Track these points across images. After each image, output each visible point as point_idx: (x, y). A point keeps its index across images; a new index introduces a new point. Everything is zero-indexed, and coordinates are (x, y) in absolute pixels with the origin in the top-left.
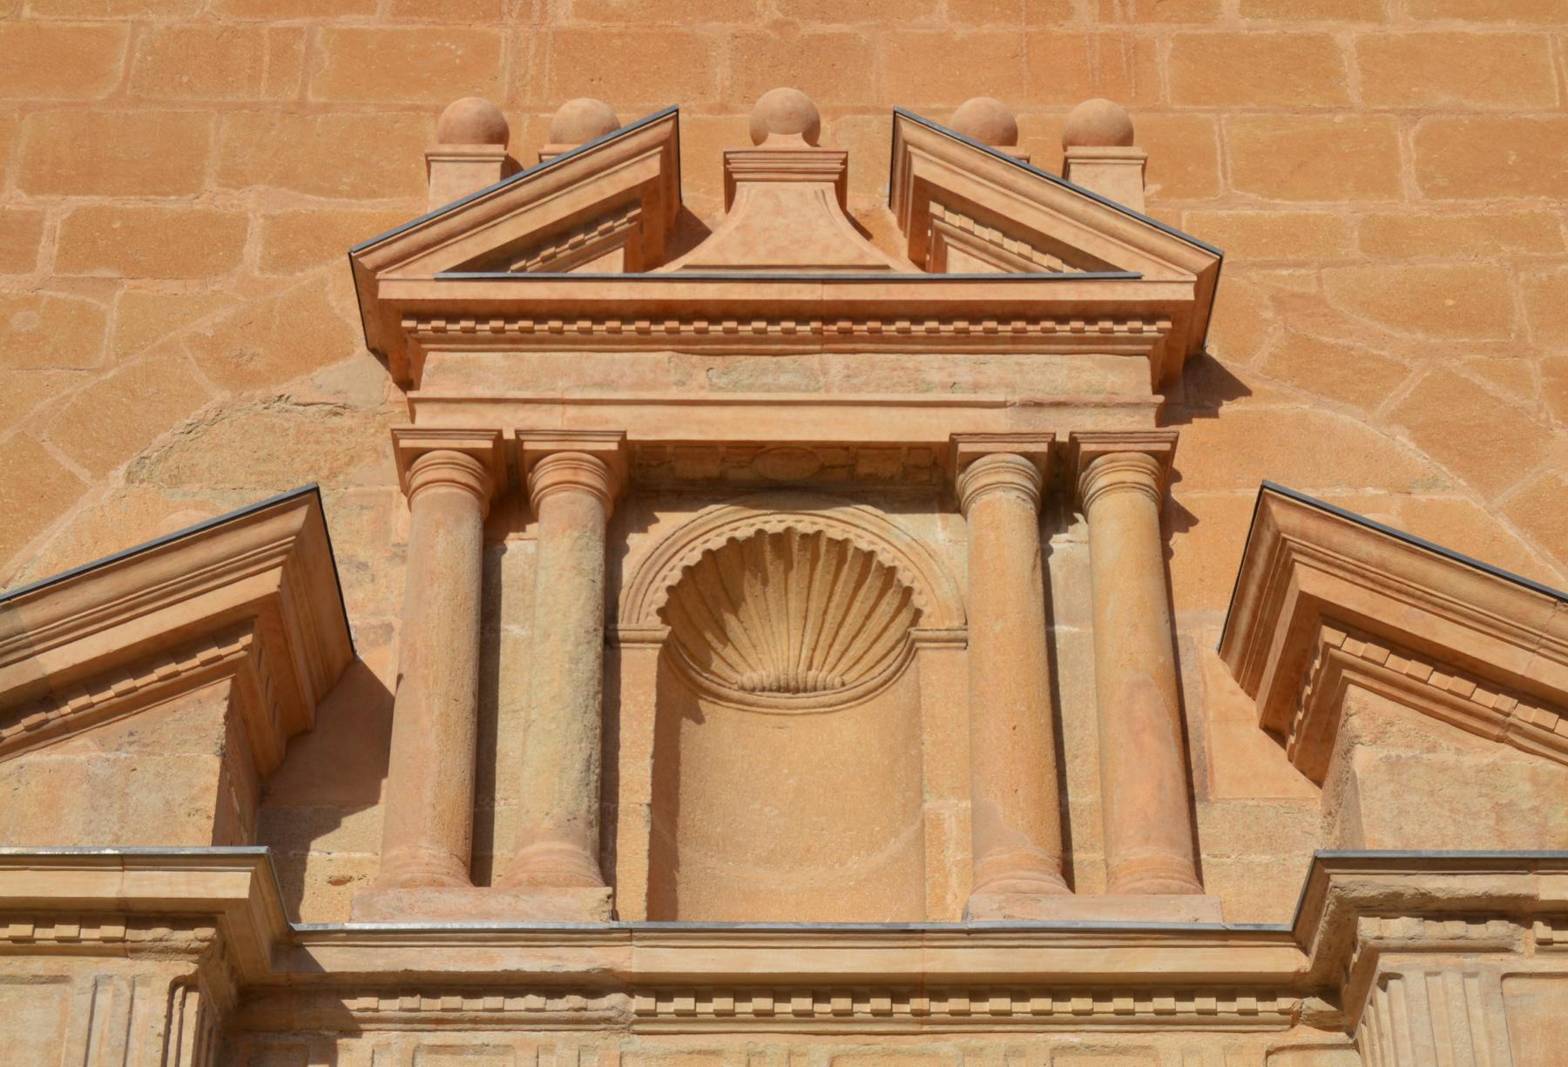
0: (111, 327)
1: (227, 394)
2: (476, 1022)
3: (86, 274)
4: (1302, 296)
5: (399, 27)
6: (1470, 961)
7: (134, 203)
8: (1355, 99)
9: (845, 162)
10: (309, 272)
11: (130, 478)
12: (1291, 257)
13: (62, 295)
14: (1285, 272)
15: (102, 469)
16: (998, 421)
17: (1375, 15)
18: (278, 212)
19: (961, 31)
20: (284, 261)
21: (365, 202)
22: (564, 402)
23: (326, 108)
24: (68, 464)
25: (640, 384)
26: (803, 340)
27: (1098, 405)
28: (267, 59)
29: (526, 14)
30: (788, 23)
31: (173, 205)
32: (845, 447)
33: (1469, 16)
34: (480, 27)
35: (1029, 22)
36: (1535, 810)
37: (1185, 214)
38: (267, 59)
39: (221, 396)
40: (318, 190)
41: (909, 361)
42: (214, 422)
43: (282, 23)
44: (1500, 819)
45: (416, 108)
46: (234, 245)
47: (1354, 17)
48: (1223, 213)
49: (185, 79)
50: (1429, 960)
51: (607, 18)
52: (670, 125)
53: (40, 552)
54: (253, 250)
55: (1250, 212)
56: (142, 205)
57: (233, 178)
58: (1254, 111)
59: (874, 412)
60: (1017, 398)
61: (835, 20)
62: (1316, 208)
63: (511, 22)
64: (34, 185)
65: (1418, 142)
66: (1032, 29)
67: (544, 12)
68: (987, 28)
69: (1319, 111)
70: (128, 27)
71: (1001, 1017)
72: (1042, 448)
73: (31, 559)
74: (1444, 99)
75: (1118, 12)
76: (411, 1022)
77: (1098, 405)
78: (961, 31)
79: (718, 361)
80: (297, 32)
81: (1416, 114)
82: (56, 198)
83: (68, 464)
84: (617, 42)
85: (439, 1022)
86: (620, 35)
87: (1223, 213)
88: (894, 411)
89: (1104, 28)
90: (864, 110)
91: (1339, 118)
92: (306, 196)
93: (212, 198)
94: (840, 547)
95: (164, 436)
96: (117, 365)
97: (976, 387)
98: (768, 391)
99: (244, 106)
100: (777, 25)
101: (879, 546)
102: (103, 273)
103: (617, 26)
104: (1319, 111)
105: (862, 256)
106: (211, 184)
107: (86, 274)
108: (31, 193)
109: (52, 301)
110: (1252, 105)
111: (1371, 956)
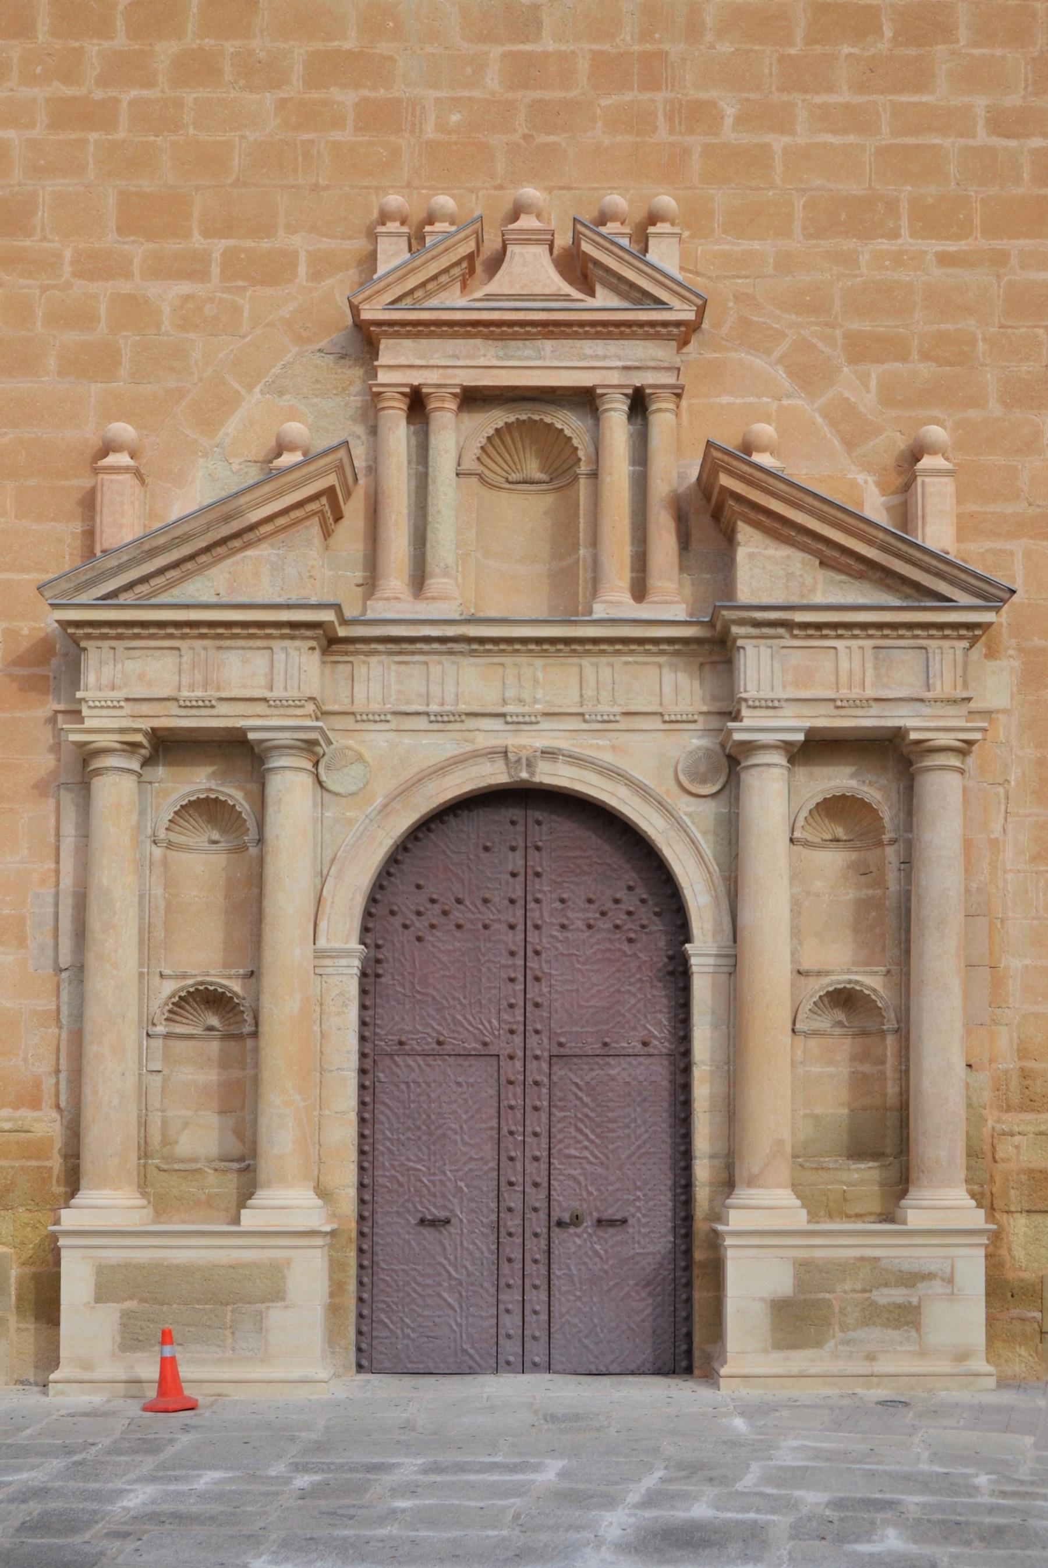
0: (246, 314)
1: (297, 349)
2: (413, 653)
3: (233, 284)
4: (746, 294)
5: (358, 139)
6: (769, 642)
7: (249, 244)
8: (778, 181)
9: (553, 235)
10: (327, 282)
11: (262, 392)
12: (744, 273)
13: (224, 296)
14: (740, 281)
15: (250, 388)
16: (615, 378)
17: (792, 132)
18: (310, 248)
19: (606, 141)
20: (316, 276)
21: (348, 242)
22: (438, 367)
23: (327, 188)
24: (236, 386)
25: (467, 357)
26: (534, 334)
27: (654, 368)
28: (300, 158)
29: (412, 131)
30: (531, 136)
31: (266, 245)
32: (552, 388)
33: (835, 132)
34: (393, 139)
35: (637, 135)
36: (801, 576)
37: (700, 249)
38: (300, 158)
39: (294, 350)
40: (327, 236)
41: (578, 343)
42: (292, 363)
43: (306, 137)
44: (788, 581)
45: (367, 187)
46: (294, 266)
47: (783, 132)
48: (716, 248)
49: (265, 171)
50: (754, 641)
51: (450, 133)
52: (479, 224)
53: (230, 431)
54: (302, 270)
55: (728, 247)
56: (253, 245)
57: (291, 229)
58: (732, 189)
59: (563, 371)
60: (620, 364)
61: (550, 134)
62: (756, 245)
63: (407, 135)
64: (207, 233)
65: (804, 207)
66: (639, 139)
67: (421, 129)
68: (619, 138)
69: (761, 189)
70: (237, 139)
71: (603, 652)
72: (630, 391)
73: (228, 434)
74: (818, 182)
75: (677, 130)
76: (391, 653)
77: (654, 368)
79: (500, 343)
80: (312, 141)
81: (804, 190)
82: (216, 241)
83: (236, 386)
84: (454, 147)
85: (400, 653)
86: (456, 143)
87: (716, 248)
88: (571, 372)
89: (671, 139)
90: (563, 188)
91: (770, 194)
92: (324, 239)
93: (282, 240)
94: (550, 426)
95: (273, 371)
96: (250, 333)
97: (605, 357)
98: (520, 359)
99: (292, 187)
100: (526, 137)
101: (565, 427)
102: (240, 283)
103: (454, 138)
104: (761, 189)
105: (560, 289)
106: (281, 232)
107: (233, 284)
108: (205, 238)
109: (221, 299)
110: (733, 185)
111: (735, 640)
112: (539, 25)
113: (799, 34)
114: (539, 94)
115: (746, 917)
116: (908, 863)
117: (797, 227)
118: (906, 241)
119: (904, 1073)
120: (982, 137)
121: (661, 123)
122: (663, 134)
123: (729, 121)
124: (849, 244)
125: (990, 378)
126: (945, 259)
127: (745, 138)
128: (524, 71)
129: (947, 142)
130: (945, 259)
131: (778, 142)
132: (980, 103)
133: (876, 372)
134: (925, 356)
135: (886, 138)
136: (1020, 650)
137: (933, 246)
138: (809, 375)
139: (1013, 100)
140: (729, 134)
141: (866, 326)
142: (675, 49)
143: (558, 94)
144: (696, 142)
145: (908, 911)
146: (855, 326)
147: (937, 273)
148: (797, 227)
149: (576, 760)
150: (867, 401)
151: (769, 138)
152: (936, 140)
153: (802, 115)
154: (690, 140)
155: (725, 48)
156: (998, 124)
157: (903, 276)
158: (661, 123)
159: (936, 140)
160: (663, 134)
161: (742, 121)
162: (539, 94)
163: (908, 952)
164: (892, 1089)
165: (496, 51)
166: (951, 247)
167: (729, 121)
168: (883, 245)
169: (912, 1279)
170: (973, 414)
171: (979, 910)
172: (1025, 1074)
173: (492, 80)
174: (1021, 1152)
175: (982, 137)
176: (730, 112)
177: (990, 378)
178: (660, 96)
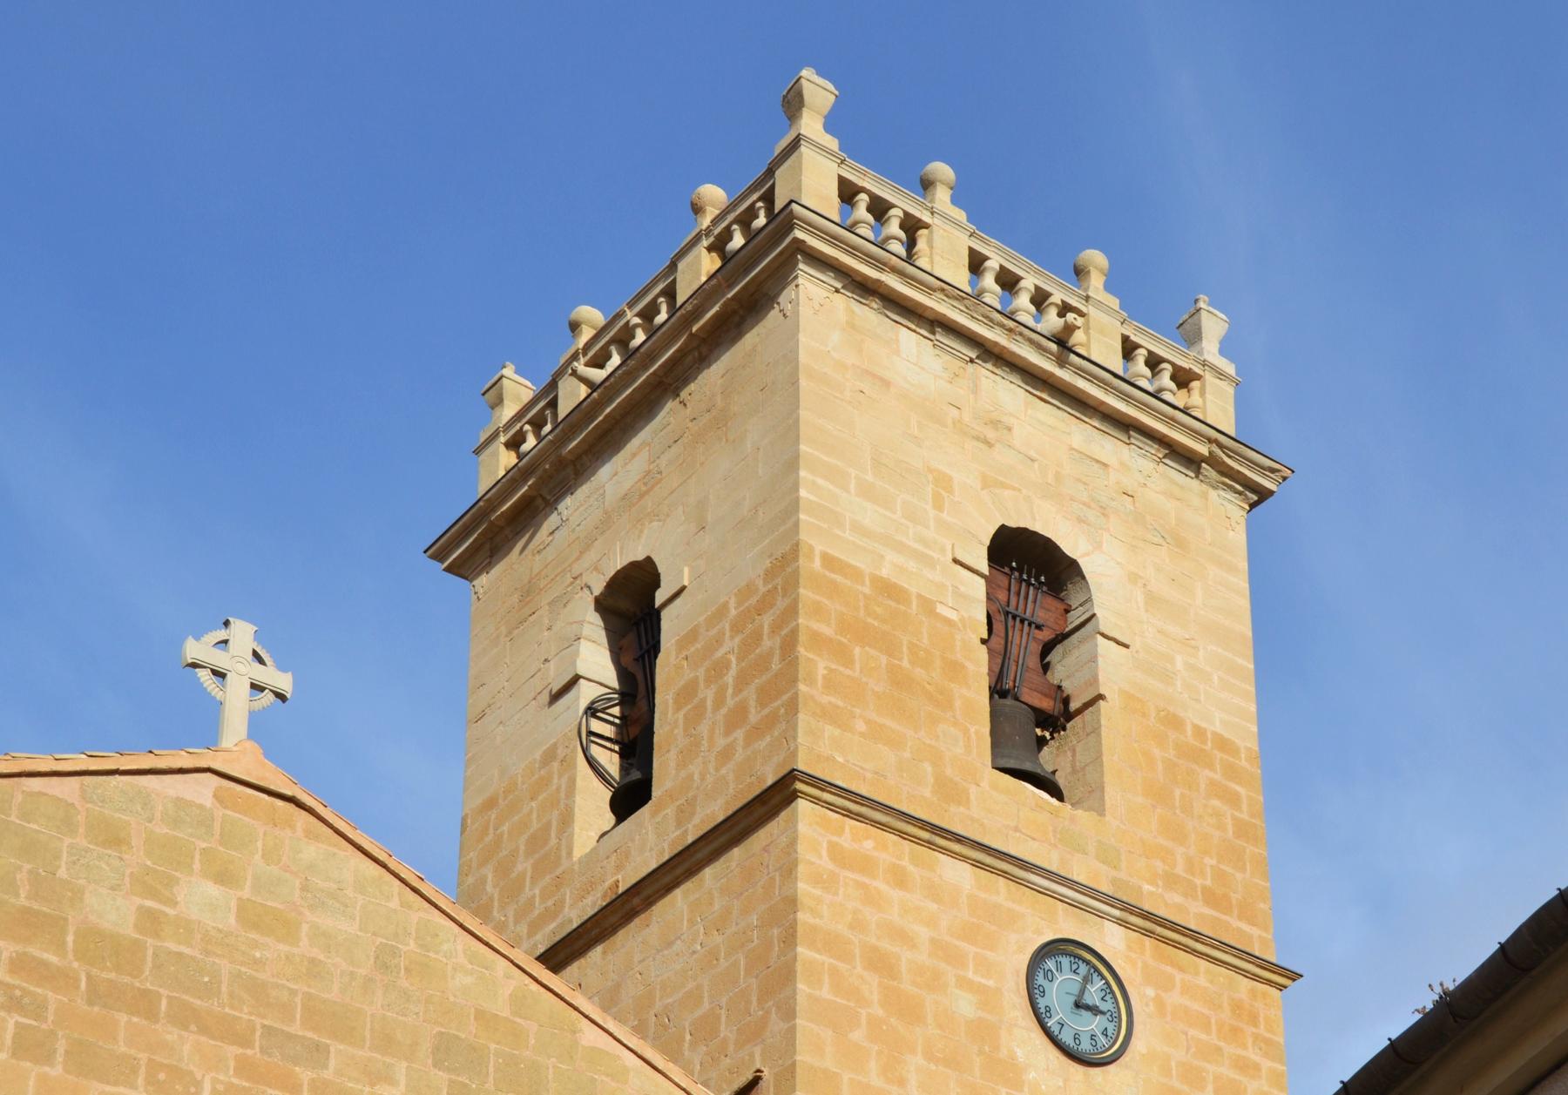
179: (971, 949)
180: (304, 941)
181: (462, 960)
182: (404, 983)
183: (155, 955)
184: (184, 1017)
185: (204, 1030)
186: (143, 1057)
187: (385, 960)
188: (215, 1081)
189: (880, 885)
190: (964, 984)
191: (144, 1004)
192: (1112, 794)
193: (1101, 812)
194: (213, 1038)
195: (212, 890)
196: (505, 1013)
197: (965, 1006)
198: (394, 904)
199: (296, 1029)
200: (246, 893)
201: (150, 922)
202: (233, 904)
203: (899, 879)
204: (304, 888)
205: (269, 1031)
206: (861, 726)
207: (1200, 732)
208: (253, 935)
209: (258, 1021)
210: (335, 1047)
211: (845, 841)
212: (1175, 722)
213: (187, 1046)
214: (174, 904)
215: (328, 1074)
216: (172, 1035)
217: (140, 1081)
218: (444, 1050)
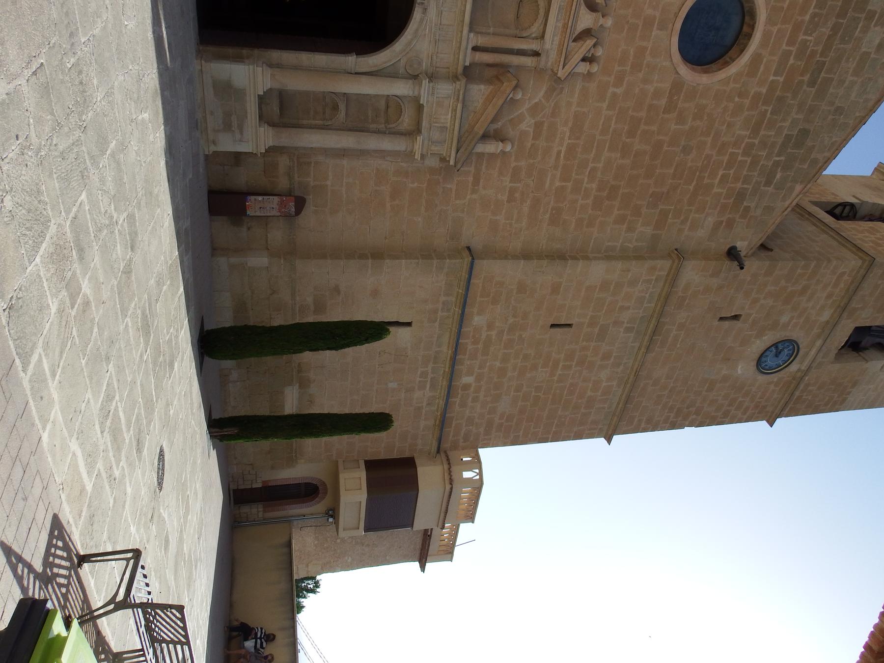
19: (620, 50)
62: (576, 96)
78: (620, 50)
112: (661, 30)
113: (634, 114)
114: (640, 28)
115: (364, 78)
116: (378, 132)
117: (579, 109)
118: (567, 141)
119: (311, 127)
120: (591, 165)
121: (621, 68)
122: (617, 68)
123: (615, 90)
124: (570, 124)
125: (523, 163)
126: (559, 152)
127: (609, 95)
128: (649, 23)
129: (592, 155)
130: (559, 152)
131: (605, 105)
132: (601, 165)
133: (531, 130)
134: (533, 145)
135: (598, 137)
136: (441, 168)
137: (564, 149)
138: (534, 110)
139: (599, 174)
140: (611, 90)
141: (545, 128)
142: (641, 75)
143: (638, 34)
144: (612, 79)
145: (363, 131)
146: (546, 124)
147: (555, 150)
148: (579, 109)
149: (422, 20)
150: (523, 126)
151: (607, 102)
152: (594, 151)
153: (611, 113)
154: (613, 77)
155: (637, 91)
156: (594, 170)
157: (557, 140)
158: (621, 68)
159: (594, 151)
160: (617, 68)
161: (614, 94)
162: (640, 28)
163: (350, 130)
164: (305, 122)
165: (658, 14)
166: (562, 155)
167: (615, 90)
168: (568, 134)
169: (241, 128)
170: (513, 158)
171: (362, 153)
172: (309, 163)
173: (649, 12)
174: (284, 162)
175: (591, 165)
176: (619, 91)
177: (523, 163)
178: (628, 68)
179: (802, 320)
180: (852, 78)
181: (834, 140)
182: (830, 117)
183: (858, 18)
184: (835, 29)
185: (830, 37)
186: (824, 12)
187: (839, 110)
188: (811, 41)
189: (829, 289)
190: (792, 318)
191: (842, 14)
192: (837, 366)
193: (832, 363)
194: (827, 40)
195: (877, 41)
196: (812, 157)
197: (784, 319)
198: (857, 114)
199: (823, 75)
200: (872, 56)
201: (871, 15)
202: (870, 50)
203: (829, 296)
204: (870, 79)
205: (824, 63)
206: (880, 282)
207: (849, 393)
208: (858, 58)
209: (828, 59)
210: (813, 90)
211: (846, 277)
212: (855, 384)
213: (826, 31)
214: (875, 26)
215: (805, 87)
216: (830, 24)
217: (817, 10)
218: (804, 133)
